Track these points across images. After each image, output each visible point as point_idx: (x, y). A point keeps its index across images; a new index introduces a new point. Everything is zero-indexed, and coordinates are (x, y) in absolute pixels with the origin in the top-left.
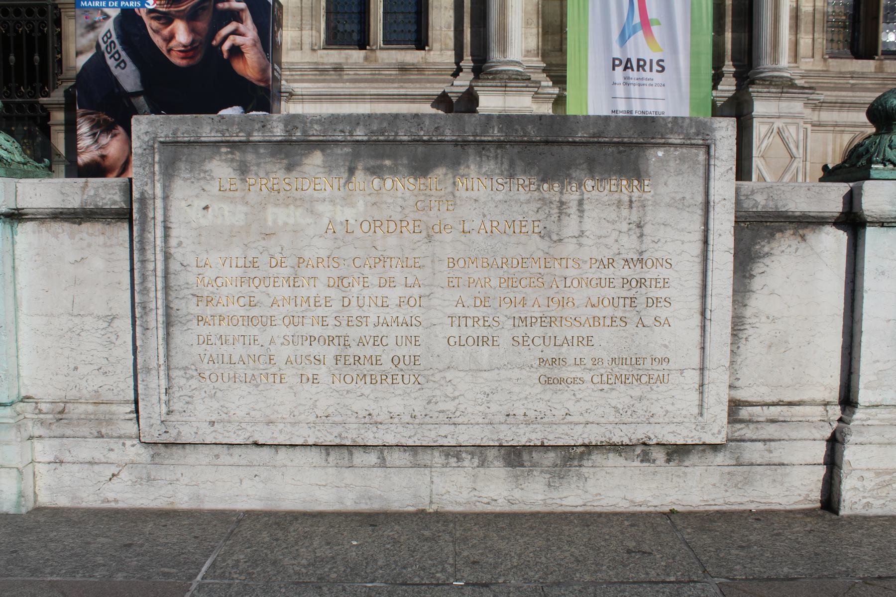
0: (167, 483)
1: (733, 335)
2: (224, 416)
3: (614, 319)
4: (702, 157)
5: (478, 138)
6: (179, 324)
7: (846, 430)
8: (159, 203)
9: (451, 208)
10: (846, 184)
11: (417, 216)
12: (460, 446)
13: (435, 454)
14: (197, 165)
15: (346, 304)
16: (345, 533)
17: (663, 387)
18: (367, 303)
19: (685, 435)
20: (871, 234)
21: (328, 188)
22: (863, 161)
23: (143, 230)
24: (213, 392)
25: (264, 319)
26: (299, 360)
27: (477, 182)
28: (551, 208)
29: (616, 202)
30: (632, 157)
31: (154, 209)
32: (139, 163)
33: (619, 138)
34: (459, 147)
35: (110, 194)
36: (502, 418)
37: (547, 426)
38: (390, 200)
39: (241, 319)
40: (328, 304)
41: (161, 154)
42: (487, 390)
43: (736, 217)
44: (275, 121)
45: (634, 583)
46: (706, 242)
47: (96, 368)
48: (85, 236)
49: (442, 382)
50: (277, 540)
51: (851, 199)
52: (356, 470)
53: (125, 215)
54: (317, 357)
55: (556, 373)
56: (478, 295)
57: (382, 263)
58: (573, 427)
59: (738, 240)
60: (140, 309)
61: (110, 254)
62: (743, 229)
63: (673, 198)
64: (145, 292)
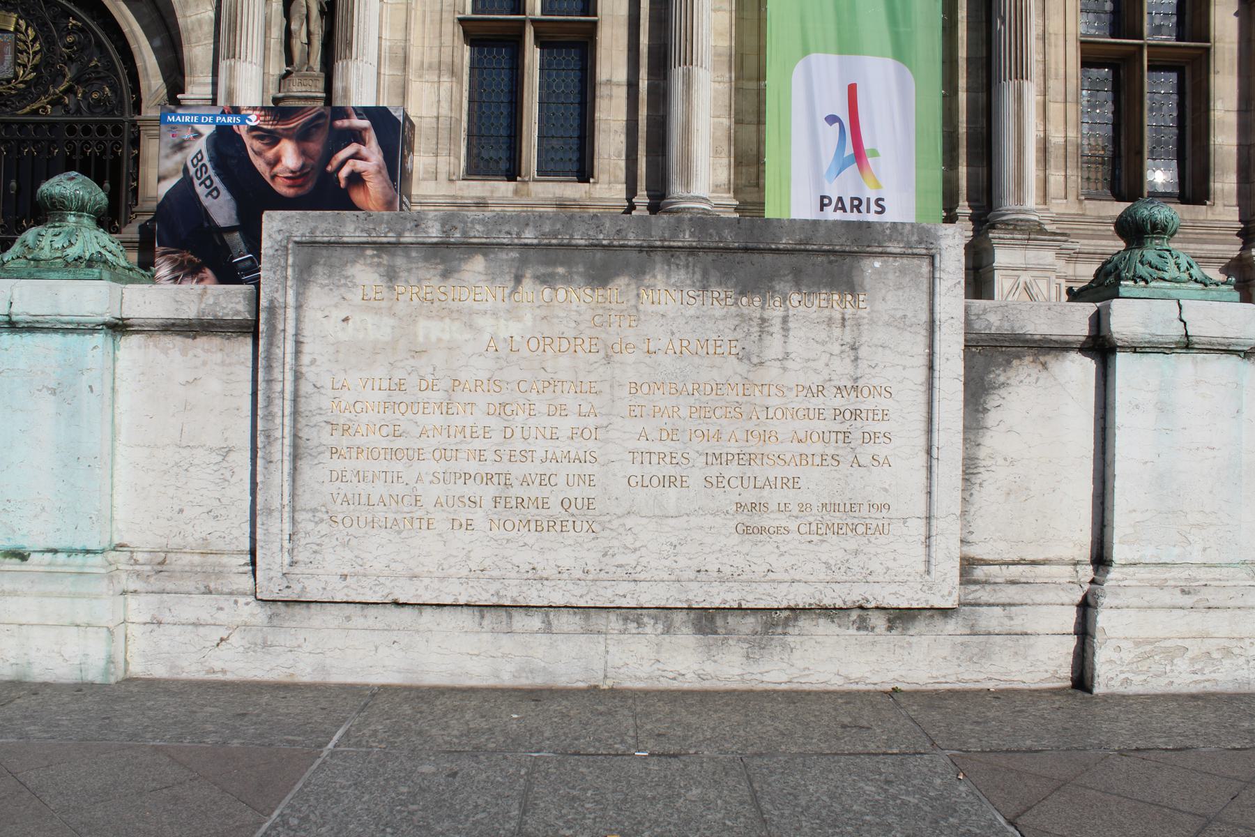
1: (965, 480)
2: (358, 568)
3: (825, 457)
4: (925, 268)
6: (309, 457)
7: (1099, 592)
8: (291, 313)
9: (633, 324)
10: (1092, 304)
11: (594, 333)
12: (642, 608)
16: (503, 707)
17: (882, 539)
20: (1122, 361)
21: (491, 299)
22: (1111, 279)
23: (270, 344)
25: (410, 452)
26: (450, 503)
29: (826, 320)
31: (285, 320)
36: (692, 575)
38: (562, 314)
40: (487, 435)
41: (295, 255)
43: (965, 340)
44: (430, 220)
45: (850, 754)
46: (931, 367)
47: (206, 510)
48: (199, 351)
49: (621, 530)
50: (421, 712)
51: (1098, 321)
52: (516, 637)
53: (249, 328)
54: (472, 499)
55: (756, 521)
58: (776, 585)
59: (968, 368)
62: (974, 354)
63: (893, 316)
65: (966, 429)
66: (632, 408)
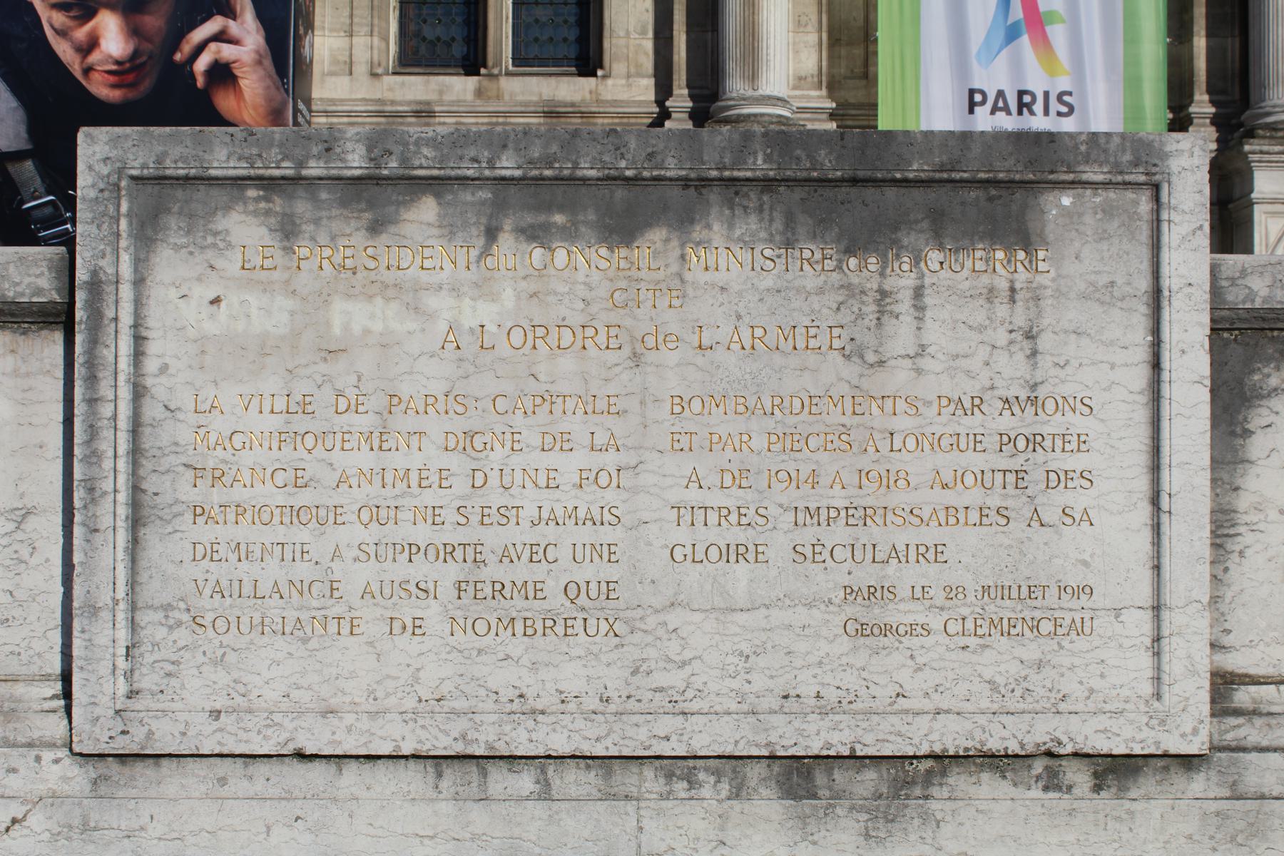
0: (121, 834)
2: (239, 699)
3: (985, 512)
4: (1144, 205)
5: (727, 174)
6: (158, 522)
8: (126, 292)
9: (676, 302)
11: (613, 318)
12: (695, 757)
13: (646, 773)
14: (202, 222)
15: (478, 483)
17: (1081, 643)
18: (518, 481)
19: (1129, 736)
21: (448, 265)
23: (94, 342)
24: (220, 652)
25: (322, 512)
26: (387, 591)
27: (724, 255)
28: (863, 303)
29: (985, 291)
30: (1014, 207)
31: (117, 302)
32: (90, 215)
33: (989, 171)
34: (692, 190)
35: (29, 276)
36: (775, 703)
37: (861, 717)
38: (563, 288)
39: (277, 512)
42: (745, 647)
43: (1212, 320)
44: (350, 140)
46: (1156, 365)
49: (661, 632)
52: (494, 806)
54: (422, 585)
55: (877, 614)
56: (728, 466)
57: (547, 406)
58: (910, 718)
60: (82, 491)
61: (24, 391)
62: (1226, 343)
64: (94, 460)
65: (1216, 463)
66: (676, 437)
